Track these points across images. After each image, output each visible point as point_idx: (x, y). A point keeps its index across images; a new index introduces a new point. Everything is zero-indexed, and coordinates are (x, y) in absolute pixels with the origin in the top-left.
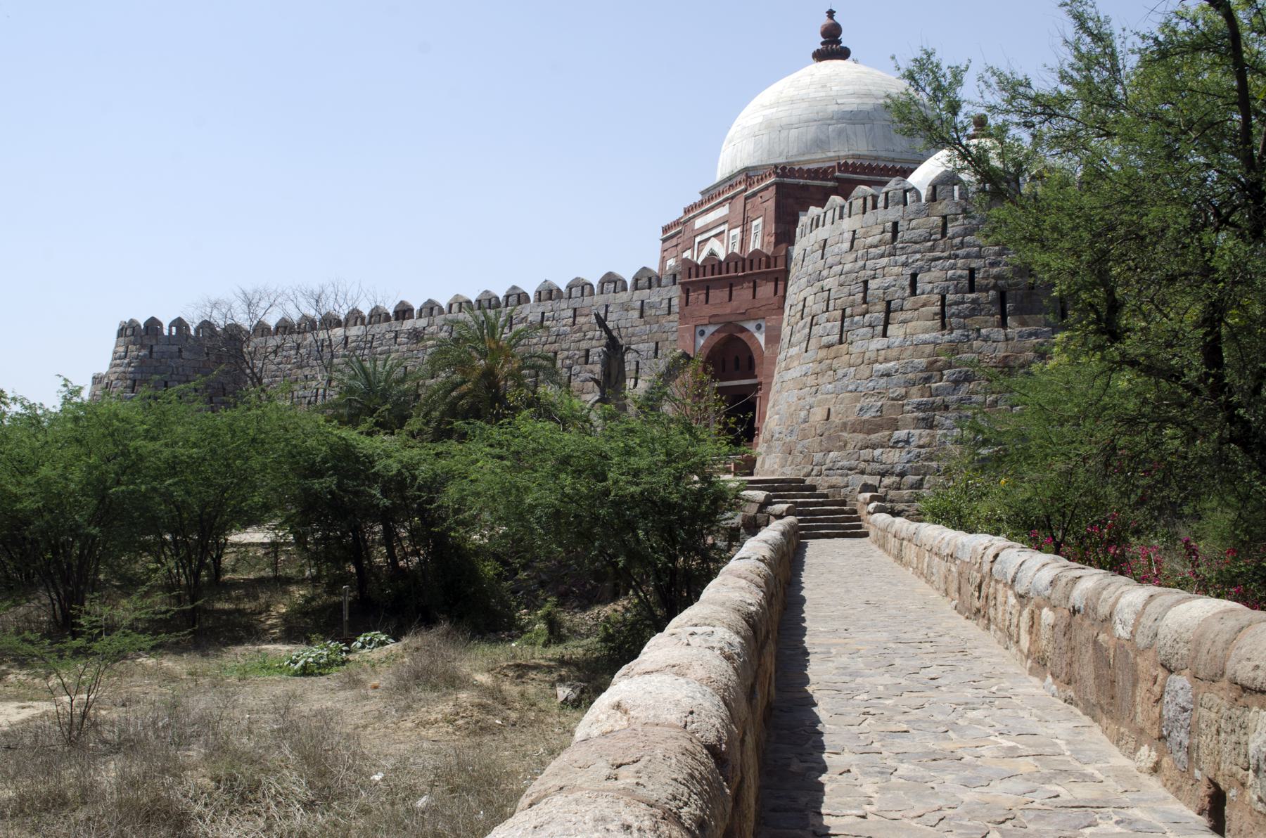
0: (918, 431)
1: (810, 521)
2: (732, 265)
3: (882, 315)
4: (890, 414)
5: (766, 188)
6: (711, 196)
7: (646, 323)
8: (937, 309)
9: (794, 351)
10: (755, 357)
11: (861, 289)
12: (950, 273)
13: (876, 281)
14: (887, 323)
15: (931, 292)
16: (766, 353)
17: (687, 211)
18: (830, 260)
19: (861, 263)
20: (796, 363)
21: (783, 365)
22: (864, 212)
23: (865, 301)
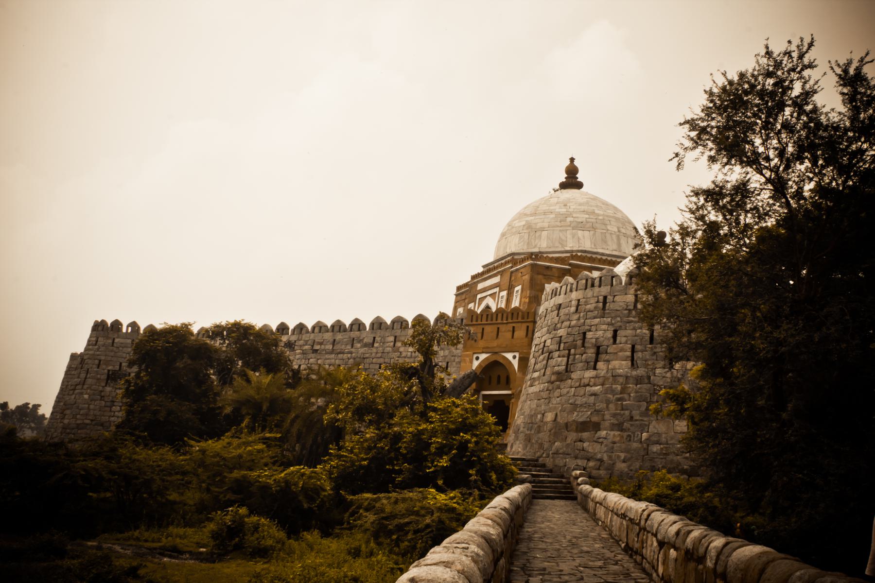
0: (612, 433)
2: (500, 315)
3: (594, 355)
4: (595, 419)
5: (525, 266)
6: (489, 270)
8: (629, 354)
9: (536, 375)
10: (511, 377)
11: (581, 337)
12: (639, 331)
13: (591, 333)
14: (596, 361)
15: (626, 343)
17: (473, 277)
18: (563, 318)
19: (582, 321)
20: (537, 383)
21: (529, 383)
22: (586, 289)
23: (583, 346)
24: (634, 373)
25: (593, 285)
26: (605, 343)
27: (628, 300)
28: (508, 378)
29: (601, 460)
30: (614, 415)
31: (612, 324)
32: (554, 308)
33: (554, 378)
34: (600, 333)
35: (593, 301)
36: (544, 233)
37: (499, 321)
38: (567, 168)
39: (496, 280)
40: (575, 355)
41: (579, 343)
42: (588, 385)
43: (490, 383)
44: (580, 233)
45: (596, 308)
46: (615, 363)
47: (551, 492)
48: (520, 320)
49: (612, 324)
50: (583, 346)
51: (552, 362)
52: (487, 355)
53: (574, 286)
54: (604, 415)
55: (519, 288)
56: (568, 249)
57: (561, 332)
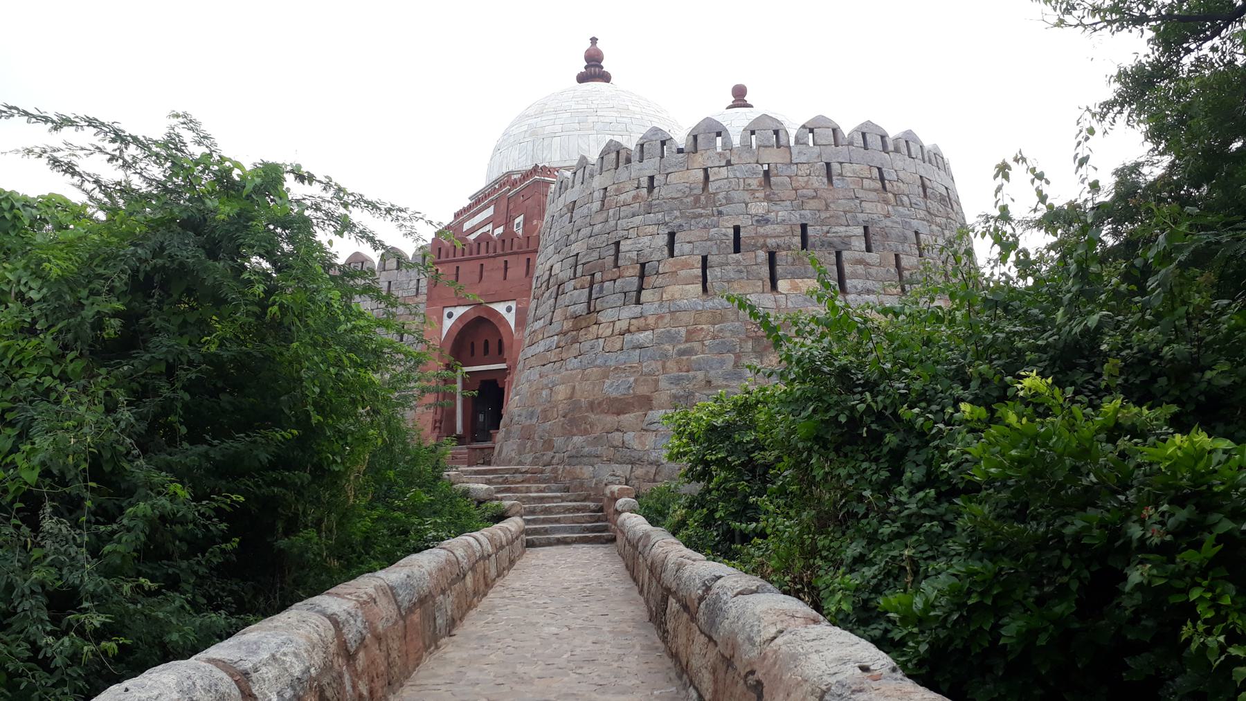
1: (544, 521)
2: (483, 245)
3: (636, 280)
4: (643, 390)
6: (479, 201)
8: (699, 272)
10: (505, 340)
11: (612, 252)
13: (629, 242)
14: (640, 289)
15: (691, 254)
16: (516, 336)
17: (457, 215)
18: (579, 223)
19: (612, 223)
23: (616, 266)
24: (710, 304)
25: (628, 161)
26: (656, 257)
30: (677, 381)
31: (666, 224)
33: (568, 325)
34: (646, 239)
35: (630, 186)
39: (489, 212)
42: (628, 331)
43: (473, 354)
45: (635, 198)
46: (674, 290)
47: (565, 530)
48: (515, 249)
49: (666, 224)
50: (616, 266)
51: (564, 300)
52: (467, 309)
53: (597, 167)
54: (657, 381)
55: (520, 219)
57: (575, 248)
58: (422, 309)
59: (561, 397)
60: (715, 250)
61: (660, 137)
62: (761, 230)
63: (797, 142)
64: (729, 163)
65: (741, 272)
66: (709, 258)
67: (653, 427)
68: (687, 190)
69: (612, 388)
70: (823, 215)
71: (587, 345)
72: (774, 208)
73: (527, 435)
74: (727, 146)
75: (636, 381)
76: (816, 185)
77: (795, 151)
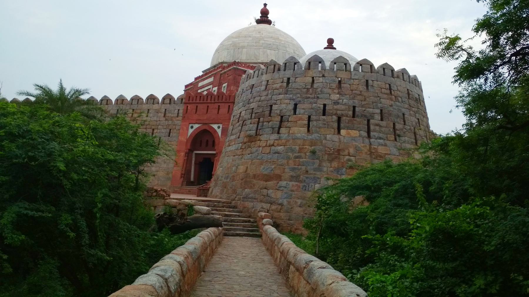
1: (231, 225)
2: (209, 97)
3: (278, 123)
4: (277, 172)
5: (230, 70)
6: (207, 73)
7: (166, 120)
8: (306, 122)
9: (233, 137)
10: (216, 141)
11: (269, 109)
13: (276, 106)
14: (280, 127)
15: (304, 114)
16: (221, 139)
17: (196, 79)
18: (254, 94)
21: (227, 144)
24: (310, 137)
26: (288, 114)
27: (306, 81)
28: (214, 142)
29: (281, 205)
30: (293, 169)
31: (293, 100)
32: (249, 88)
34: (284, 106)
35: (279, 81)
36: (245, 50)
37: (209, 101)
38: (262, 10)
40: (263, 122)
41: (267, 113)
42: (273, 145)
43: (201, 146)
44: (269, 51)
45: (281, 87)
46: (295, 130)
47: (240, 230)
48: (224, 100)
49: (293, 100)
50: (270, 116)
51: (245, 128)
52: (200, 125)
53: (265, 71)
54: (284, 169)
56: (260, 61)
57: (252, 105)
58: (179, 123)
59: (241, 171)
60: (314, 113)
61: (294, 61)
62: (335, 107)
63: (355, 69)
64: (323, 76)
65: (325, 124)
66: (311, 117)
67: (282, 188)
68: (304, 86)
69: (264, 170)
70: (363, 103)
71: (254, 149)
72: (342, 98)
73: (225, 186)
74: (323, 68)
75: (275, 168)
76: (361, 89)
77: (353, 74)
